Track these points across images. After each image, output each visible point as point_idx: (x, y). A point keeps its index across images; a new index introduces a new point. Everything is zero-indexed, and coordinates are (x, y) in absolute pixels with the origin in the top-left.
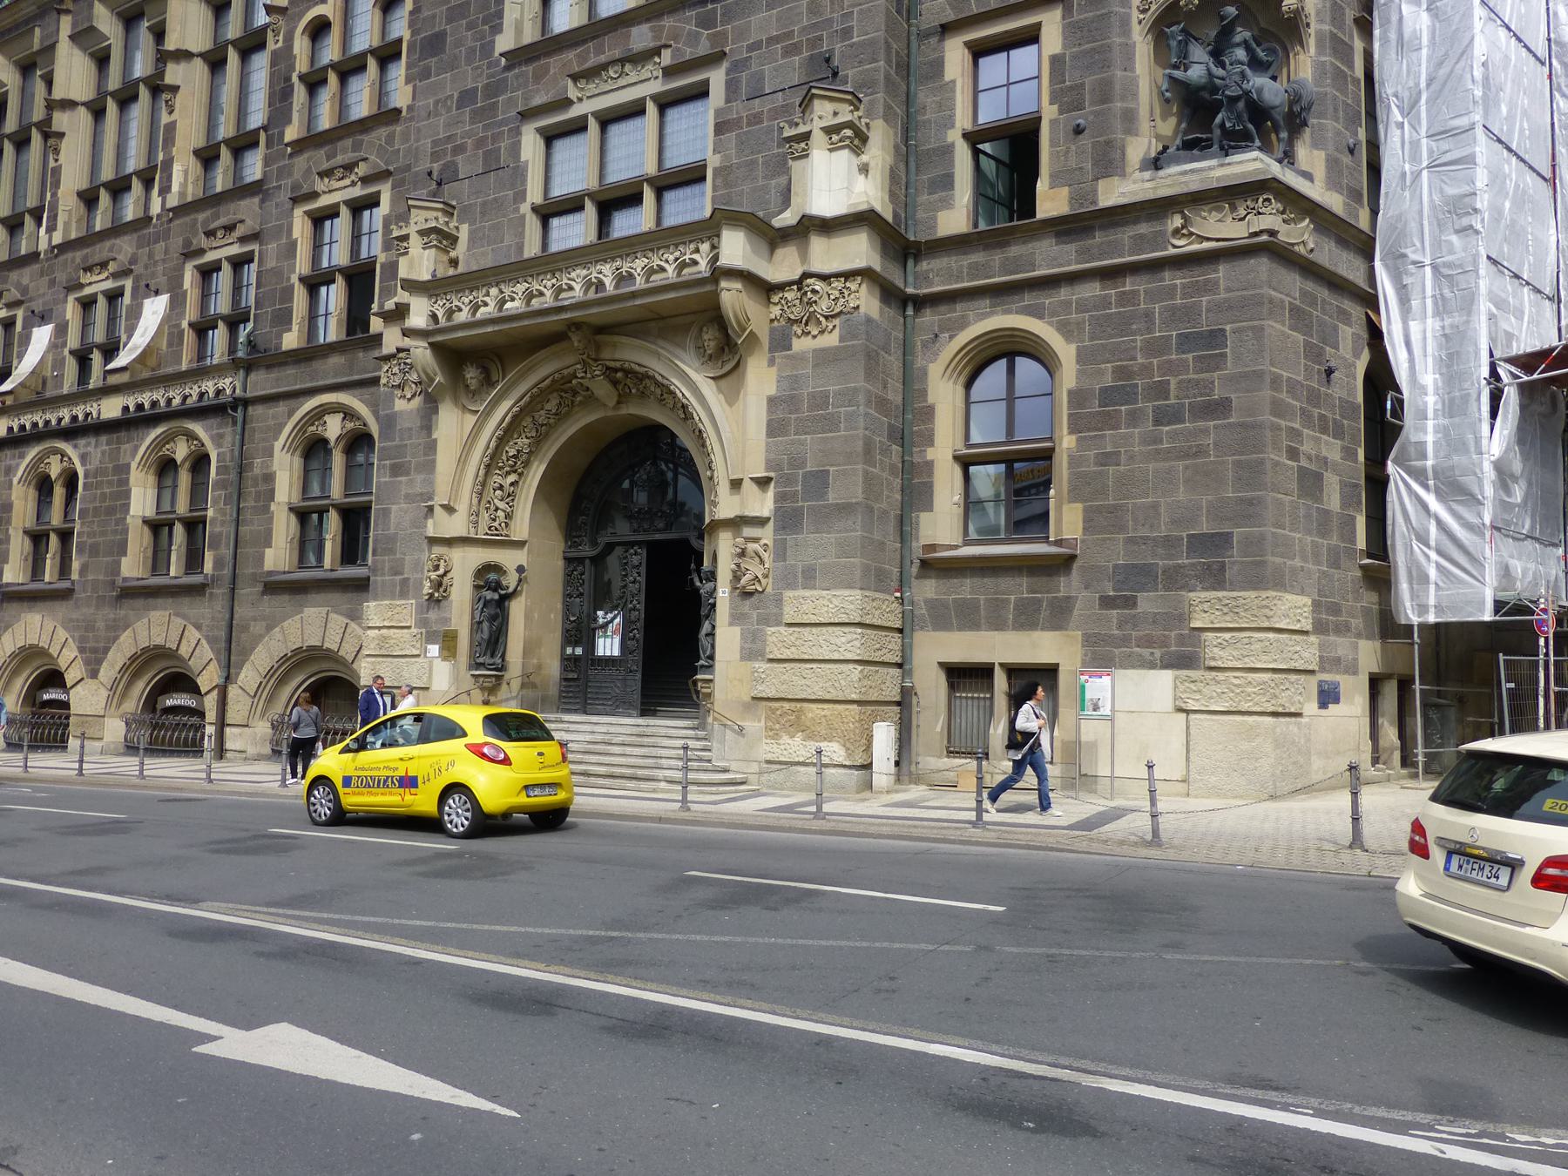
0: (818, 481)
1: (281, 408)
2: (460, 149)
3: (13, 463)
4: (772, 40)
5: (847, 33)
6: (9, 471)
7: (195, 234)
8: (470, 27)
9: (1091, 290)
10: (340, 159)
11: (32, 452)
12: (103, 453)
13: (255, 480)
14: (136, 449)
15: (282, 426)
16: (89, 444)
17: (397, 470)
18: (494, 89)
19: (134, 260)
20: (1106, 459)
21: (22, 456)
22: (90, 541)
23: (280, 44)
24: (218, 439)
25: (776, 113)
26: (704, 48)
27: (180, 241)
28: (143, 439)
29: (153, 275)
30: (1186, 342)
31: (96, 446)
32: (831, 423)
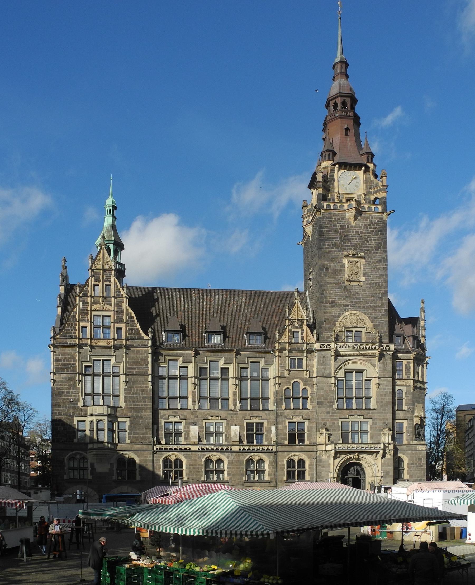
0: (388, 473)
1: (286, 453)
2: (328, 420)
3: (202, 456)
4: (378, 418)
5: (388, 420)
6: (200, 458)
7: (246, 416)
8: (328, 402)
9: (410, 452)
10: (296, 414)
11: (208, 454)
12: (234, 457)
13: (280, 465)
14: (245, 457)
15: (286, 457)
16: (228, 455)
17: (323, 467)
18: (334, 413)
19: (226, 417)
20: (411, 471)
21: (205, 455)
22: (232, 473)
23: (279, 390)
24: (269, 458)
25: (379, 427)
26: (368, 417)
27: (241, 417)
28: (247, 455)
29: (233, 422)
30: (419, 459)
31: (232, 455)
32: (390, 466)
